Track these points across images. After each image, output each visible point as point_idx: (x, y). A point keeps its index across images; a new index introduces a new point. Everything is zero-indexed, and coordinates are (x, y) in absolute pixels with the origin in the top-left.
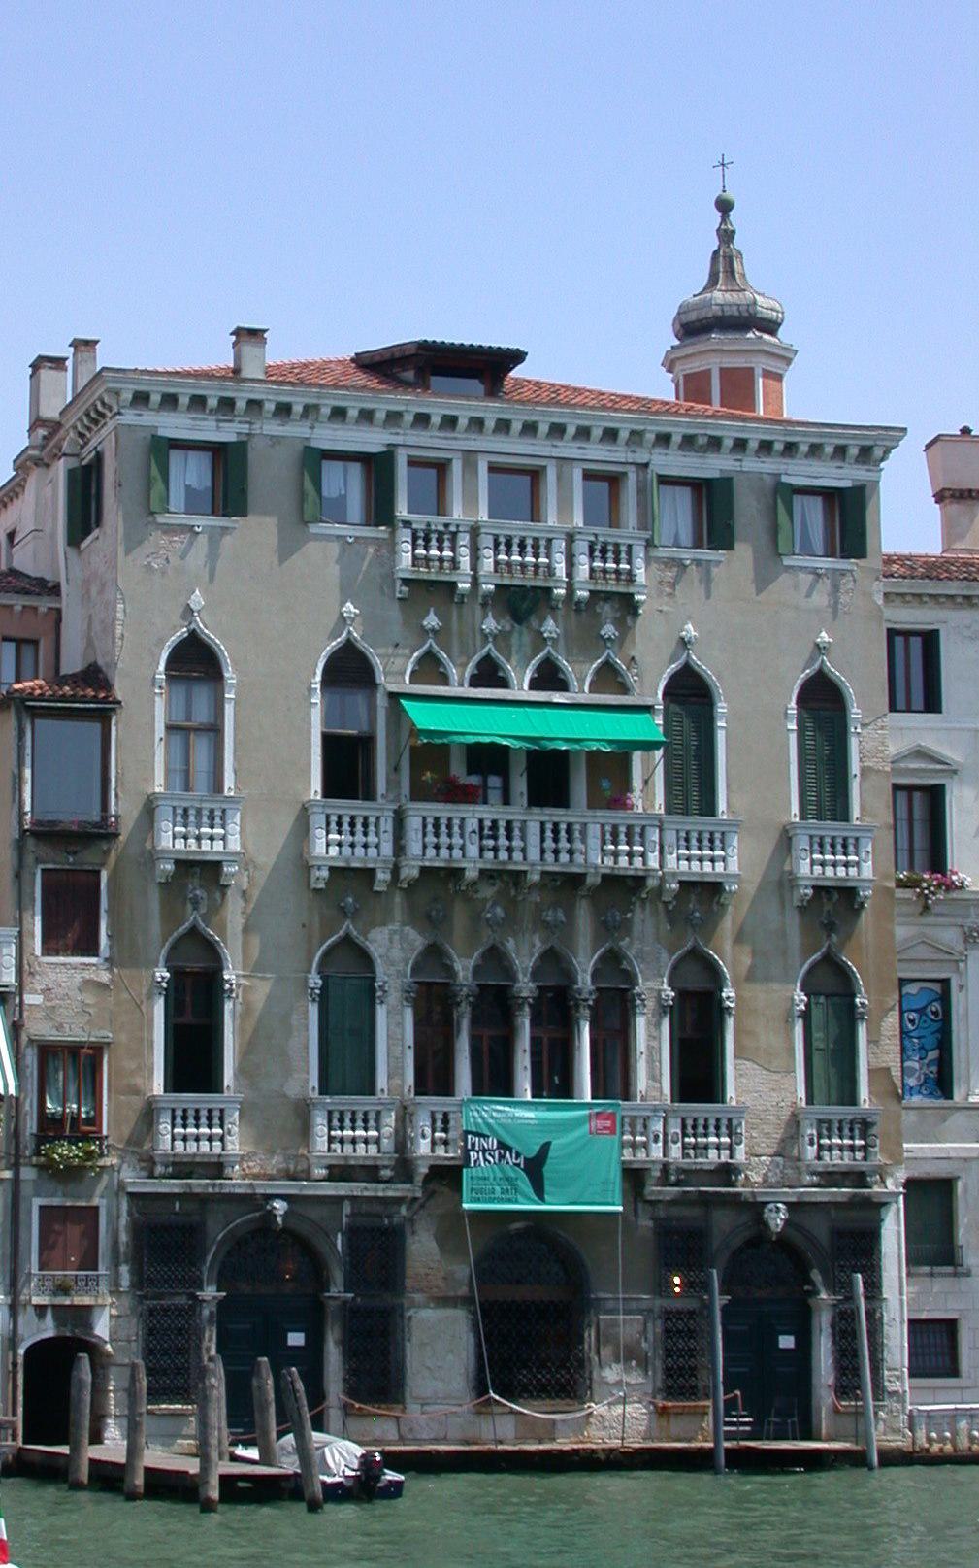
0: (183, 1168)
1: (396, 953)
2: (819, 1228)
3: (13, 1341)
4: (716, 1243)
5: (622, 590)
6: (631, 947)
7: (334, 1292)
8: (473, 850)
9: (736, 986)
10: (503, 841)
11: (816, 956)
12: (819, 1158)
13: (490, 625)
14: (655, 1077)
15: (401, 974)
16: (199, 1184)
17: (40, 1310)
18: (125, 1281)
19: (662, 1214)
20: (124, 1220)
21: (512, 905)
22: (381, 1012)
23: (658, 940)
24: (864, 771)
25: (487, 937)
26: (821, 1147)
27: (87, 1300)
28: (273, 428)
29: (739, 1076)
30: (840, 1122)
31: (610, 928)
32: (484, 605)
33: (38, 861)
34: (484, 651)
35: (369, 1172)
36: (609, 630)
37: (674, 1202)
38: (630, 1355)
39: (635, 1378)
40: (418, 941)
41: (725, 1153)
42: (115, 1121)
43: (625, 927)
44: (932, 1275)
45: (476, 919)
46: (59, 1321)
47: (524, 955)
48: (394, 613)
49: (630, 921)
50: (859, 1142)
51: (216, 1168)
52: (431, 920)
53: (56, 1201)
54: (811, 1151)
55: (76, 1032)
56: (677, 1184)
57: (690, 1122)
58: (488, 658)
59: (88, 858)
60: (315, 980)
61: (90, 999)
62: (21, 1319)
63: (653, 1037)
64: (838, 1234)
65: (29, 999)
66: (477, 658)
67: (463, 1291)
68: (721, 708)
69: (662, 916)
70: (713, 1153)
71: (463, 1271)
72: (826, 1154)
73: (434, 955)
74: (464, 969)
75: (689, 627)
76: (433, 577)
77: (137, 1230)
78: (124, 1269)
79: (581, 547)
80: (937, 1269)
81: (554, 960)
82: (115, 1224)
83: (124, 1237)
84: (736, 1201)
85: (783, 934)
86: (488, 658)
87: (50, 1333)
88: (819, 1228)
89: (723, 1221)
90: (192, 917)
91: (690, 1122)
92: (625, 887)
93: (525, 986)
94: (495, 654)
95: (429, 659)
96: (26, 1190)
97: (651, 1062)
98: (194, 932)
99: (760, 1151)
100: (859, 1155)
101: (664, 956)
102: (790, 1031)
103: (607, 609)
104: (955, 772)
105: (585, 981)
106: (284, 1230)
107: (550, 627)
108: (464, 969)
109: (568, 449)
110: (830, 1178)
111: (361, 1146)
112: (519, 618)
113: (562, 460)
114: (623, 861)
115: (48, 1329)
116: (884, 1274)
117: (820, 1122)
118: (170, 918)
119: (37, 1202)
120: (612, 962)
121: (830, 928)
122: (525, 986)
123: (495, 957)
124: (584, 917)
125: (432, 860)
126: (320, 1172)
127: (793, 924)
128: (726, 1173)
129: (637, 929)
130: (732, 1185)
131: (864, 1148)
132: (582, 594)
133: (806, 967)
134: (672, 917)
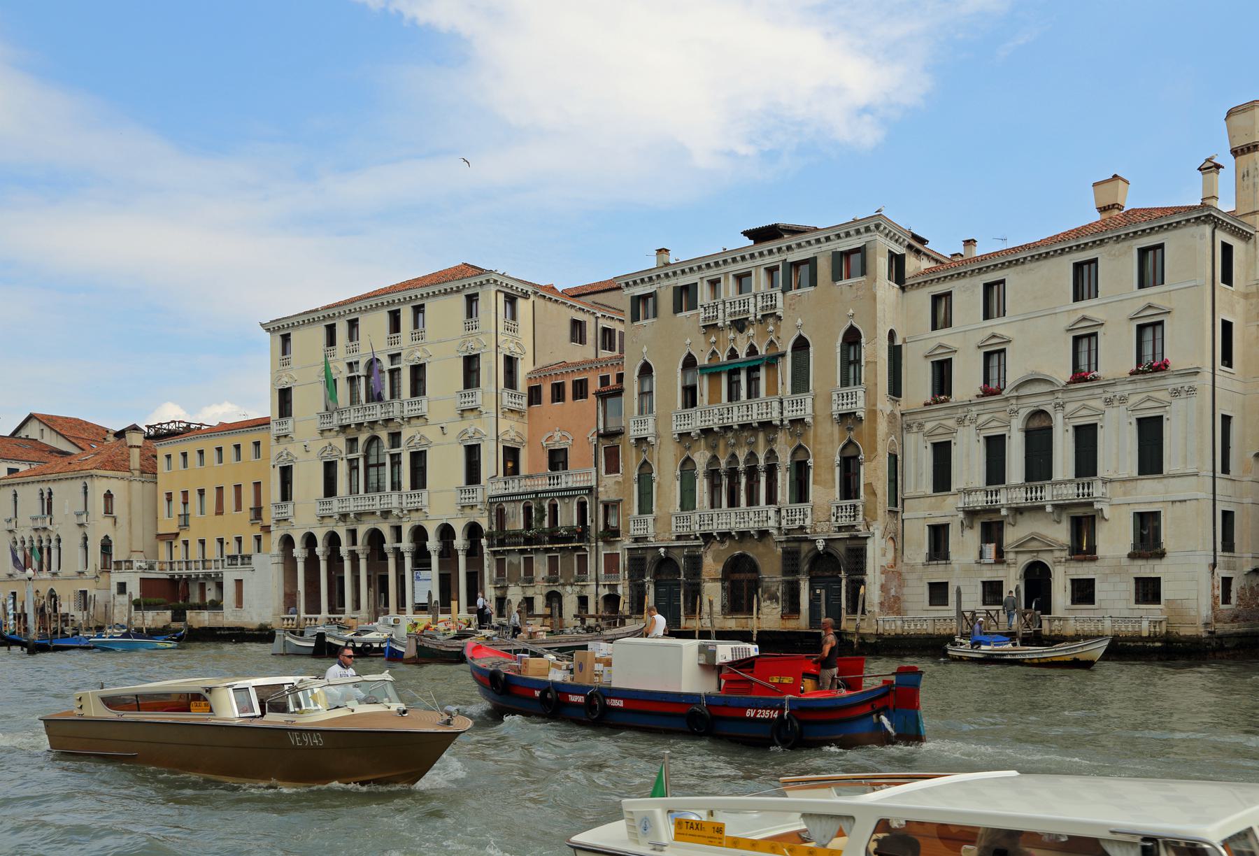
0: (637, 540)
1: (702, 461)
2: (841, 549)
3: (597, 595)
4: (803, 555)
5: (772, 311)
6: (777, 448)
7: (682, 577)
8: (716, 421)
9: (814, 457)
10: (726, 416)
11: (845, 441)
12: (837, 521)
13: (732, 335)
14: (783, 495)
15: (703, 467)
16: (641, 545)
17: (604, 585)
18: (627, 577)
19: (785, 545)
20: (626, 557)
21: (737, 439)
22: (697, 481)
23: (786, 443)
24: (867, 363)
25: (730, 450)
26: (837, 517)
27: (615, 583)
28: (665, 283)
29: (814, 492)
30: (846, 506)
31: (770, 441)
32: (730, 329)
33: (603, 445)
34: (730, 347)
35: (687, 537)
36: (771, 328)
37: (787, 541)
38: (773, 598)
39: (774, 605)
40: (708, 455)
41: (802, 522)
42: (623, 525)
43: (773, 440)
44: (937, 564)
45: (727, 445)
46: (610, 589)
47: (742, 454)
48: (702, 338)
49: (776, 438)
50: (852, 514)
51: (645, 539)
52: (714, 447)
53: (608, 552)
54: (833, 519)
55: (613, 497)
56: (786, 534)
57: (790, 511)
58: (732, 348)
59: (616, 441)
60: (678, 472)
61: (617, 487)
62: (599, 589)
63: (784, 480)
64: (849, 550)
65: (600, 489)
66: (728, 349)
67: (720, 577)
68: (811, 349)
69: (788, 434)
70: (797, 522)
71: (720, 568)
72: (839, 520)
73: (714, 459)
74: (723, 464)
75: (799, 320)
76: (710, 323)
77: (630, 559)
78: (626, 572)
79: (759, 298)
80: (939, 562)
81: (752, 455)
82: (623, 560)
83: (626, 562)
84: (806, 540)
85: (832, 434)
86: (732, 348)
87: (607, 593)
88: (841, 549)
89: (805, 547)
90: (643, 456)
91: (790, 511)
92: (766, 426)
93: (741, 467)
94: (734, 347)
95: (714, 352)
96: (600, 549)
97: (782, 490)
98: (645, 461)
99: (820, 520)
100: (852, 519)
101: (788, 449)
102: (833, 470)
103: (771, 320)
104: (956, 351)
105: (762, 463)
106: (824, 553)
107: (751, 331)
108: (723, 464)
109: (724, 269)
110: (840, 529)
111: (685, 528)
112: (741, 330)
113: (726, 274)
114: (725, 421)
115: (606, 592)
116: (868, 565)
117: (837, 507)
118: (638, 457)
119: (603, 552)
120: (772, 452)
121: (850, 429)
122: (741, 467)
123: (734, 456)
124: (761, 436)
125: (704, 425)
126: (674, 538)
127: (836, 428)
128: (802, 528)
129: (778, 440)
130: (808, 534)
131: (854, 516)
132: (759, 317)
133: (841, 446)
134: (791, 434)
